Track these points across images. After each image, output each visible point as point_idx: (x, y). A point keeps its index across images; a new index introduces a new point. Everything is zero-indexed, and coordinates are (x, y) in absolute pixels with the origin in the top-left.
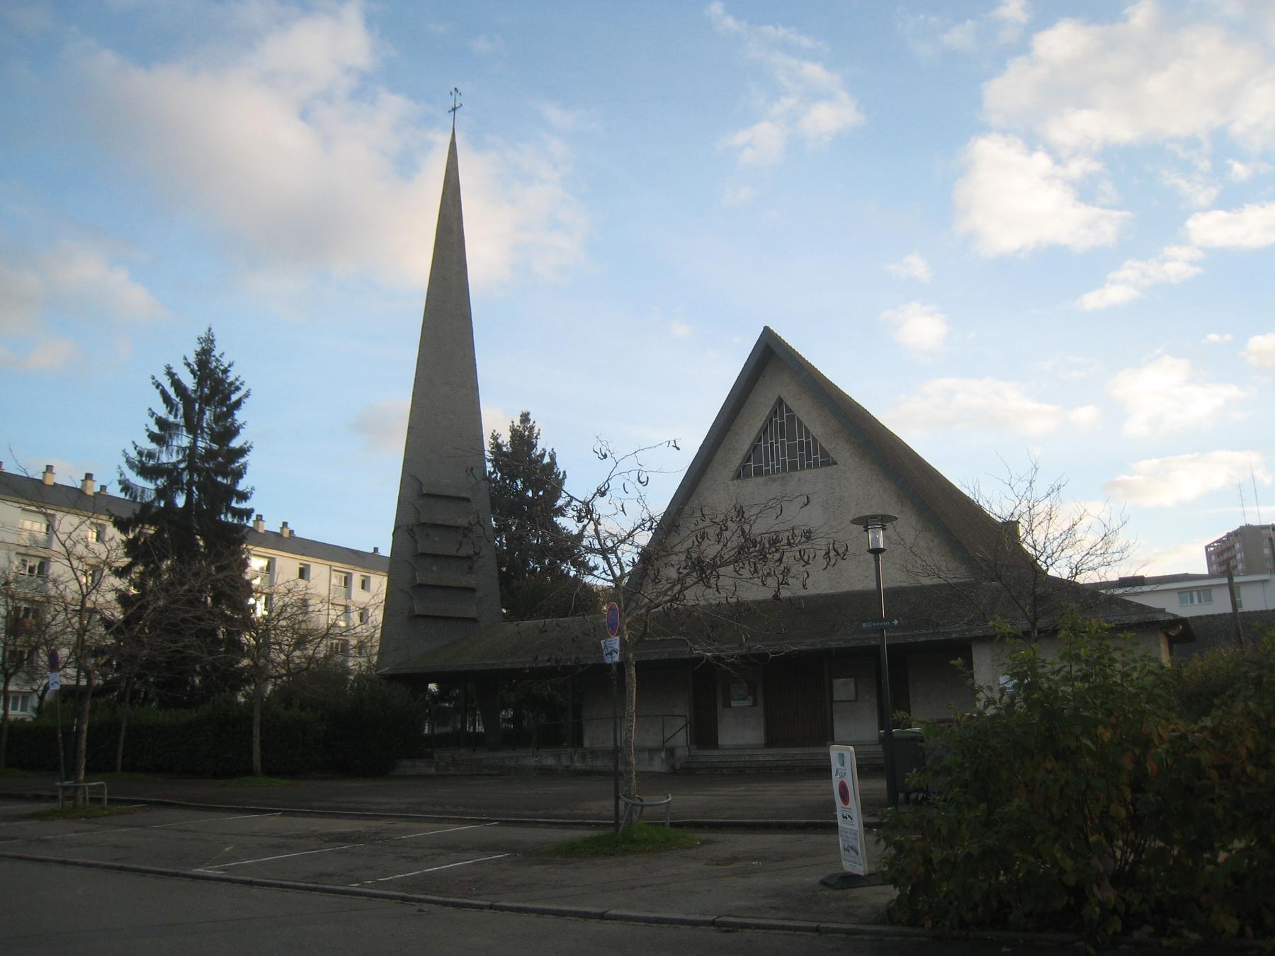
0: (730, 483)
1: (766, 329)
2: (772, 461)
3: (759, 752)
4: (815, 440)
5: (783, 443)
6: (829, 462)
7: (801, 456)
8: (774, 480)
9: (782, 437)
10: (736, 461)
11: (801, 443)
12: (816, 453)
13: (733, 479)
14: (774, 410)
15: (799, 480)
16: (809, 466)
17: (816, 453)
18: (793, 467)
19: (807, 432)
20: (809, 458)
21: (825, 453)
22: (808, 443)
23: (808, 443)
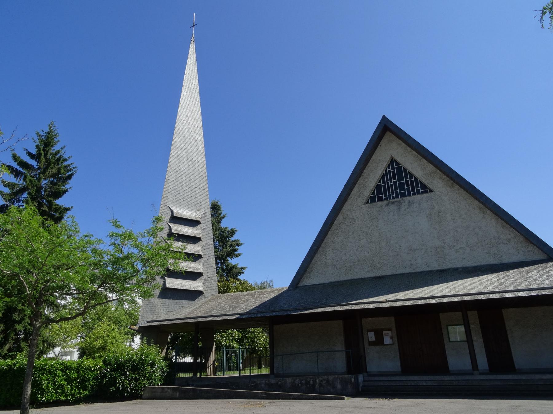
0: (363, 206)
1: (384, 117)
2: (389, 192)
3: (397, 378)
4: (416, 179)
5: (395, 183)
6: (425, 189)
7: (408, 189)
8: (393, 203)
9: (394, 178)
10: (367, 193)
11: (407, 182)
12: (417, 187)
13: (365, 204)
14: (388, 164)
15: (409, 202)
16: (414, 194)
17: (417, 187)
18: (403, 195)
19: (411, 175)
20: (413, 190)
21: (424, 186)
22: (412, 182)
23: (412, 182)
